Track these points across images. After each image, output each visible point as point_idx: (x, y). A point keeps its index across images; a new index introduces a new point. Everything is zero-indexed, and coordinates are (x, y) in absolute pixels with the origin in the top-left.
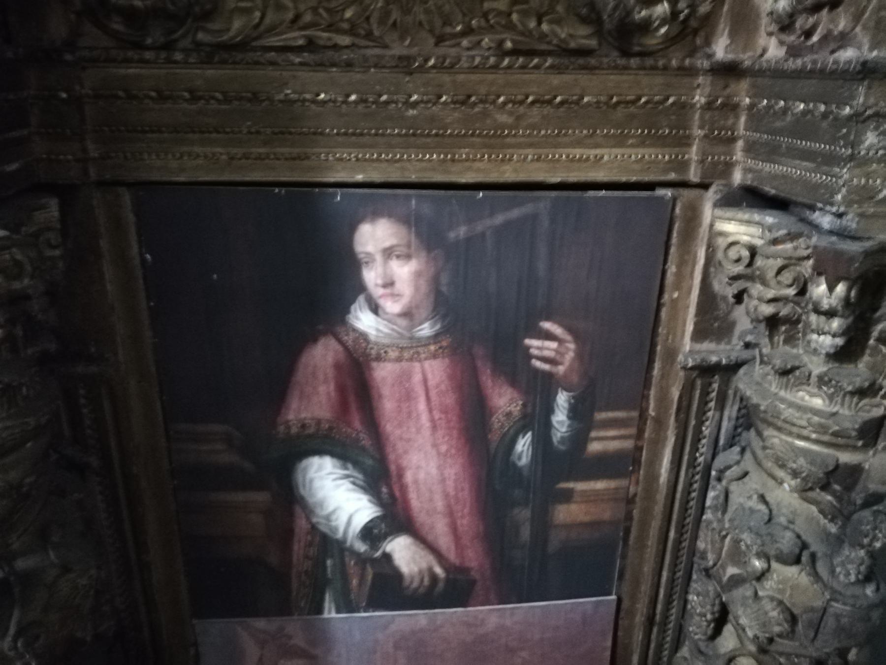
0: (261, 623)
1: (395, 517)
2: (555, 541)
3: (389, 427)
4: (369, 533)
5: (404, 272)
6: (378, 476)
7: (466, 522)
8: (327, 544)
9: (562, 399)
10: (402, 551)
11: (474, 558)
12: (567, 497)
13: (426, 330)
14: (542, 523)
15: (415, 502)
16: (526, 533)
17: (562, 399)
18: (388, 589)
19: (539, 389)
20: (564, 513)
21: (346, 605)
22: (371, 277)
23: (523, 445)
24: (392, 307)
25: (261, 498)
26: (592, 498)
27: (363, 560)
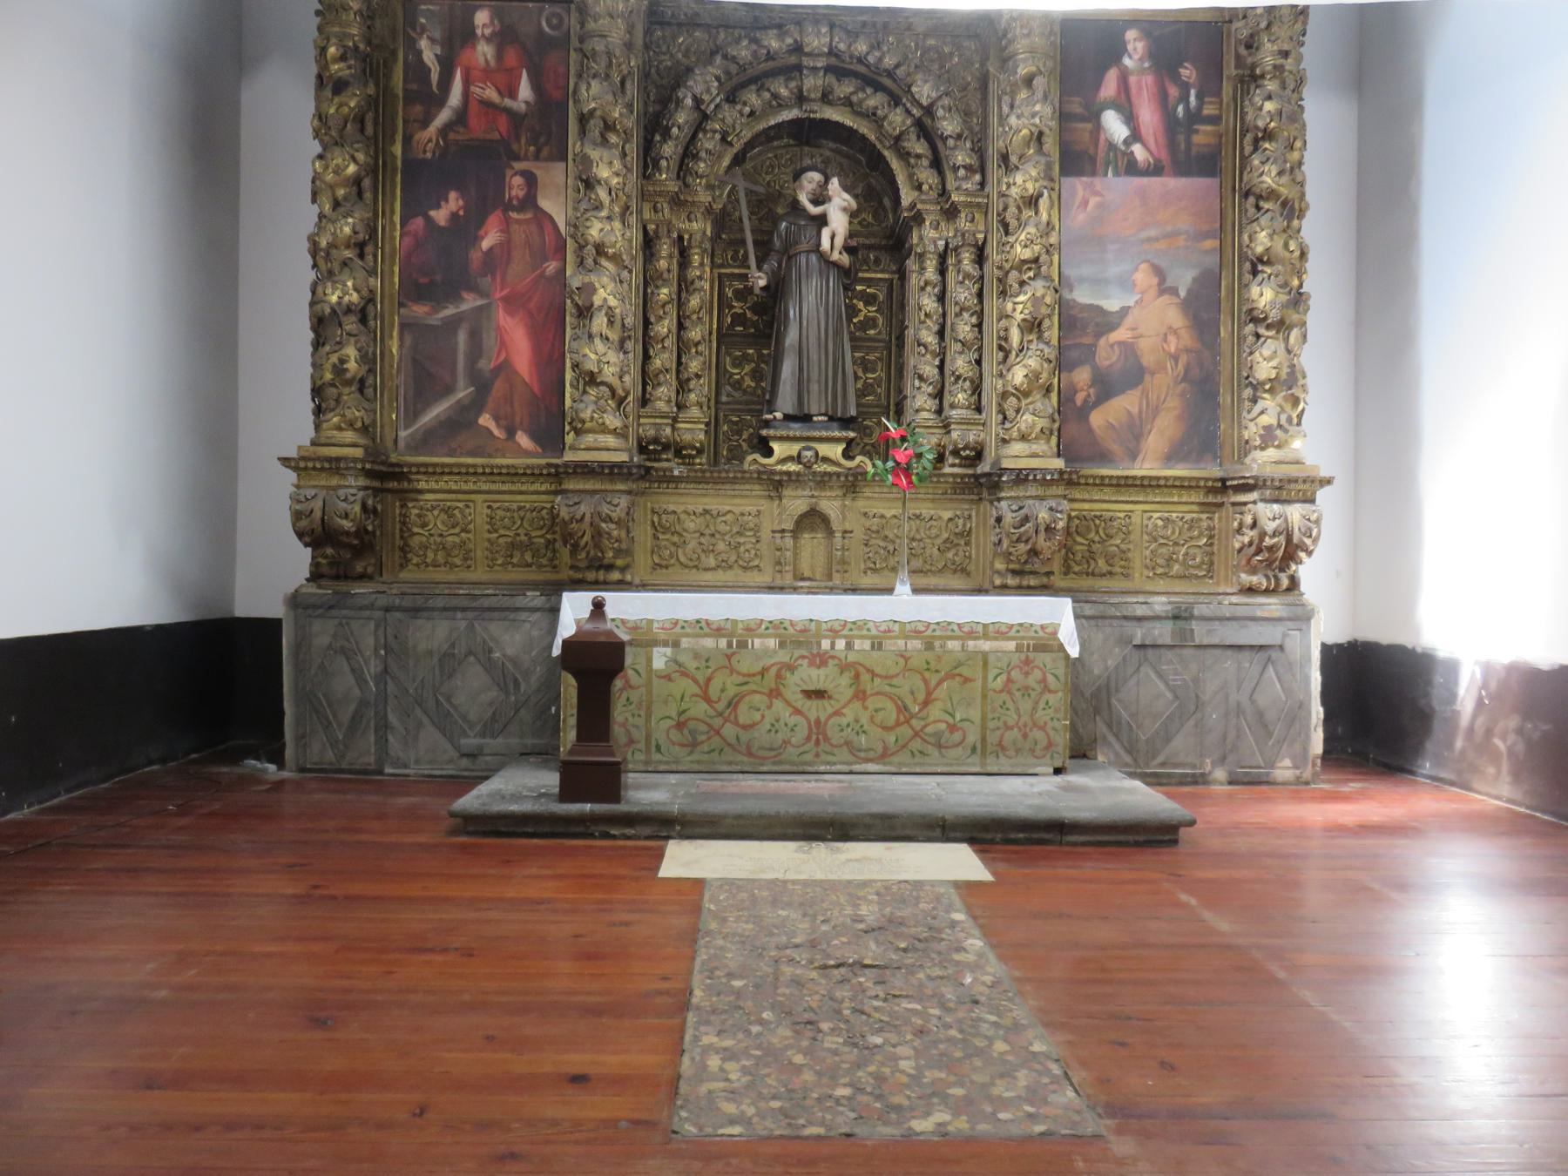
0: (1084, 179)
1: (1136, 136)
2: (1194, 151)
3: (1134, 99)
4: (1127, 142)
5: (1140, 45)
6: (1130, 119)
7: (1162, 140)
8: (1112, 146)
9: (1193, 92)
10: (1138, 151)
11: (1164, 156)
12: (1197, 131)
13: (1146, 65)
14: (1189, 143)
15: (1143, 130)
16: (1183, 147)
17: (1193, 92)
18: (1132, 168)
19: (1185, 87)
20: (1196, 139)
21: (1117, 174)
22: (1130, 47)
23: (1180, 109)
24: (1136, 57)
25: (1089, 126)
26: (1205, 132)
27: (1124, 154)
